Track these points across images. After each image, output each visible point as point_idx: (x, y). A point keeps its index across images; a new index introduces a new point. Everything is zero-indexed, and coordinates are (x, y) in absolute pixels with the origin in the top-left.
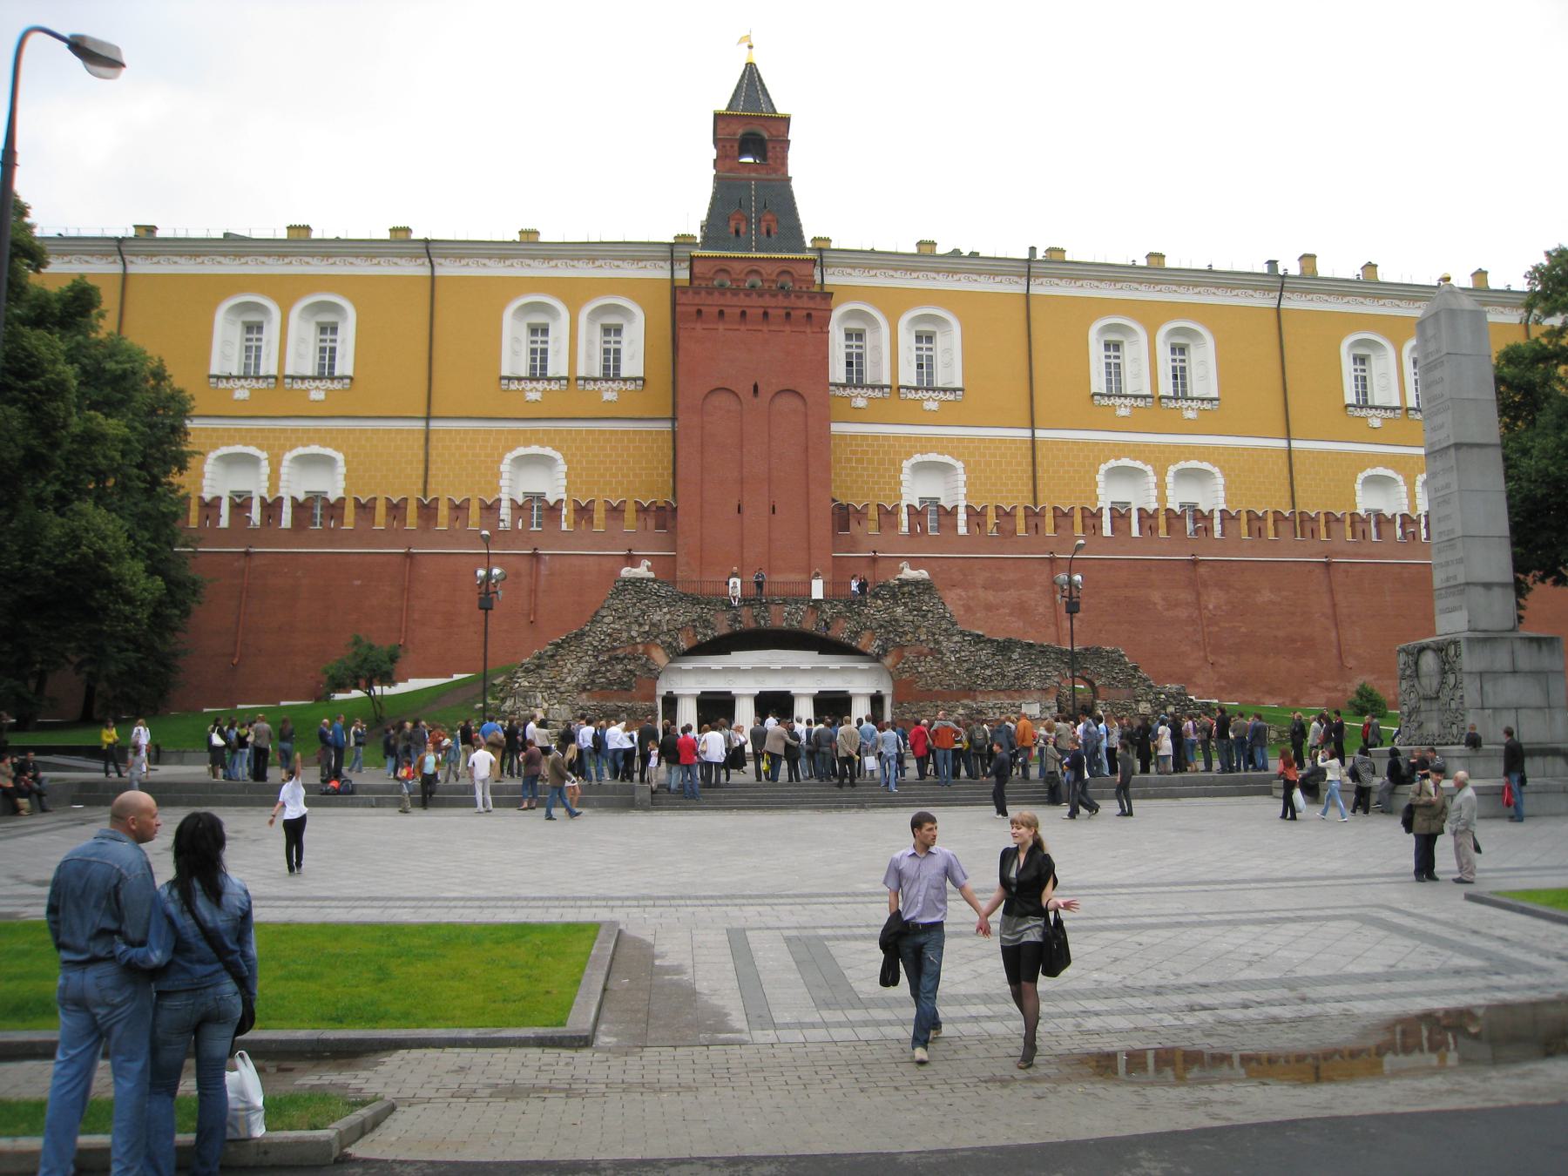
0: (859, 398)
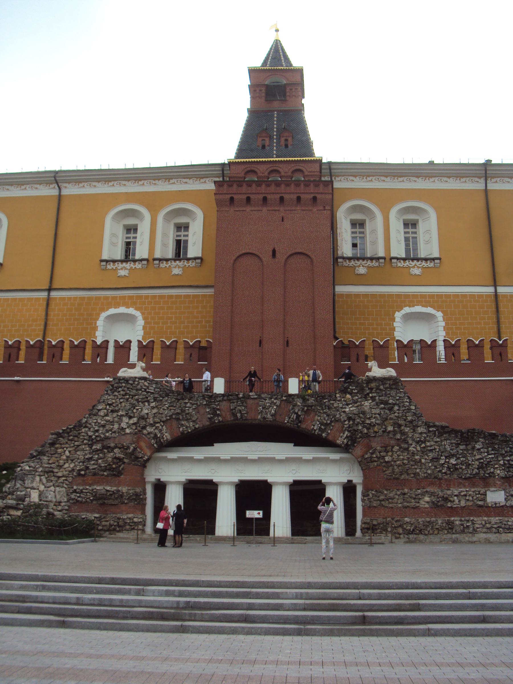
0: (361, 267)
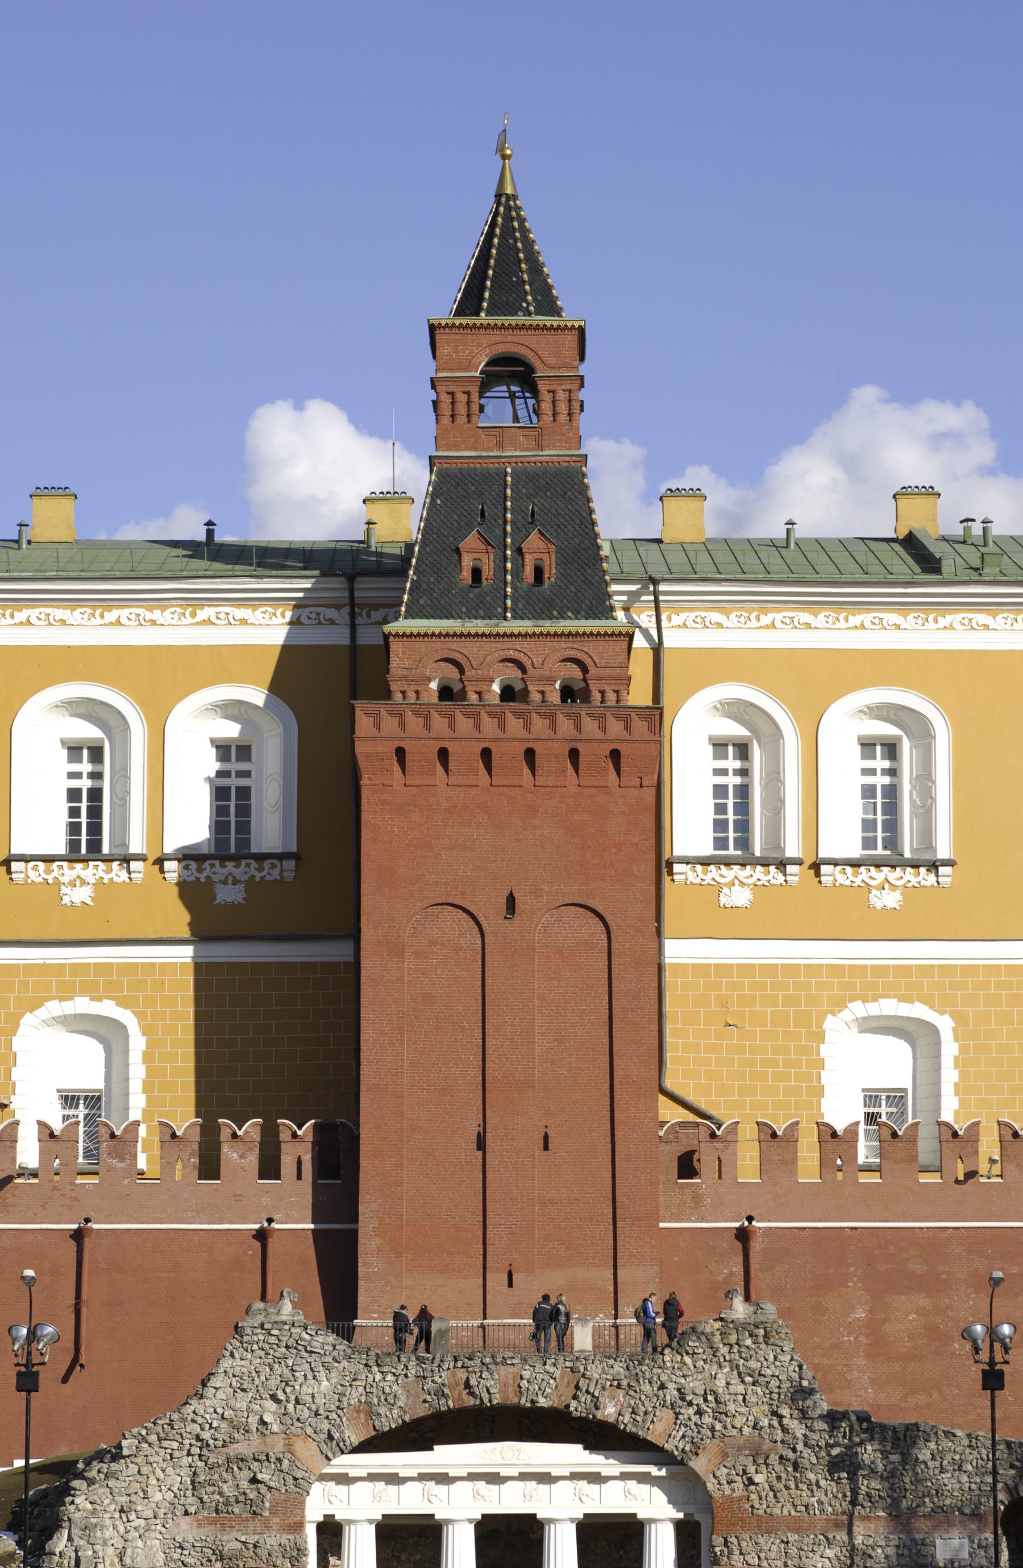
0: (737, 888)
